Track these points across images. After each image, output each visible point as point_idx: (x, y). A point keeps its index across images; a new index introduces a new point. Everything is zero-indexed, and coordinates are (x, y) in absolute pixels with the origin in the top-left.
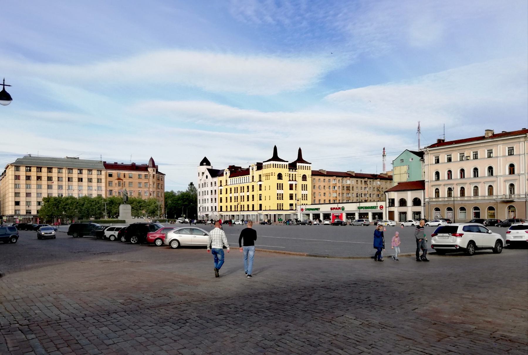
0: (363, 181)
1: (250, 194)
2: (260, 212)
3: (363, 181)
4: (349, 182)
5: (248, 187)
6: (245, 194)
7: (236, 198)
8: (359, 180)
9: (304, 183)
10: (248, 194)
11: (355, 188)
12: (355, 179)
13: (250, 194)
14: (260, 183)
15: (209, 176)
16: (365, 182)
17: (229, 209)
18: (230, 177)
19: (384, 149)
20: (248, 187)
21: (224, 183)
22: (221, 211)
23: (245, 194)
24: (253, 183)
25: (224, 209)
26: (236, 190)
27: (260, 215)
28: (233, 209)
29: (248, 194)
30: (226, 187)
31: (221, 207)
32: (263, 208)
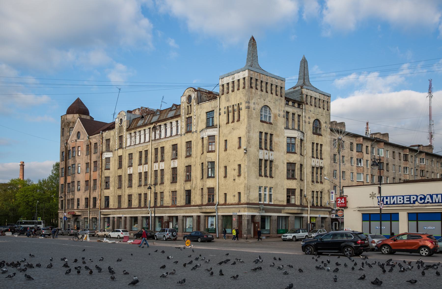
0: (402, 155)
1: (180, 164)
2: (209, 209)
3: (402, 155)
4: (382, 153)
5: (175, 147)
6: (166, 166)
7: (143, 176)
8: (397, 151)
9: (317, 139)
10: (175, 164)
11: (390, 166)
12: (391, 149)
13: (180, 164)
14: (211, 132)
15: (83, 131)
16: (406, 156)
17: (125, 204)
18: (128, 130)
19: (367, 124)
20: (175, 147)
21: (115, 143)
22: (107, 206)
23: (166, 166)
24: (189, 137)
25: (113, 203)
26: (143, 157)
27: (208, 215)
28: (135, 203)
29: (175, 164)
30: (120, 152)
31: (107, 198)
32: (218, 198)
